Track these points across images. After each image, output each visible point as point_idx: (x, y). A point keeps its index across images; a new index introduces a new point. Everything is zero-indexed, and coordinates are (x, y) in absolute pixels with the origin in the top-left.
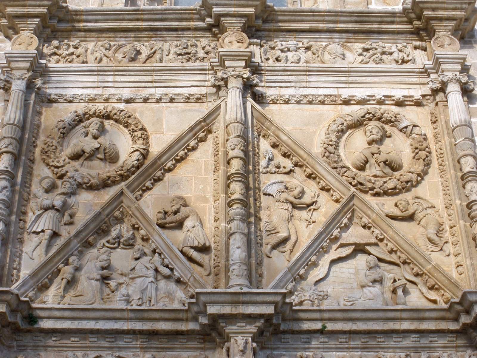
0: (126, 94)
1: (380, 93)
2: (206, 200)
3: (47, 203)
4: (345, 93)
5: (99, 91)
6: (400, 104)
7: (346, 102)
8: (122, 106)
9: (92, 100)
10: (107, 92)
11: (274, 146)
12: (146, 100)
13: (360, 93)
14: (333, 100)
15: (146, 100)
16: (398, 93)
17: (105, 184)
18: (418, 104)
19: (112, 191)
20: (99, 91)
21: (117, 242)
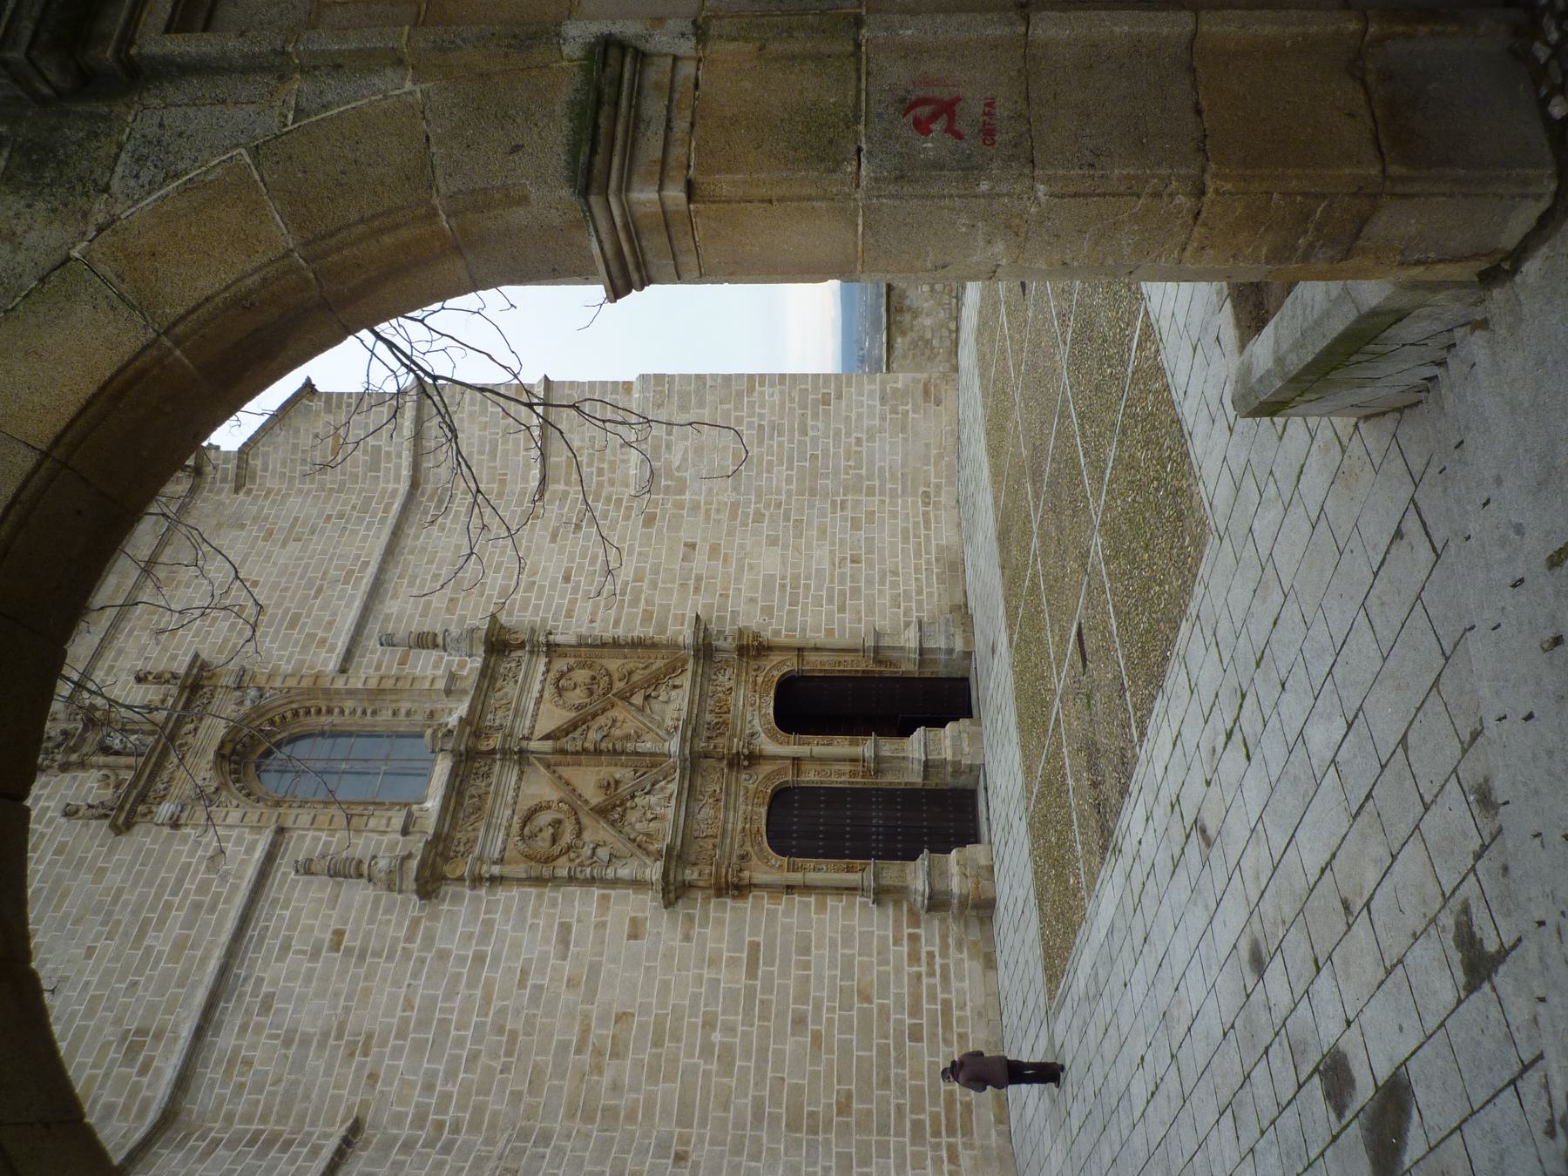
0: (508, 812)
1: (539, 677)
2: (599, 771)
3: (589, 853)
4: (536, 694)
5: (503, 829)
6: (548, 671)
7: (541, 697)
8: (516, 818)
9: (508, 835)
10: (505, 823)
11: (567, 735)
12: (515, 803)
13: (537, 687)
14: (539, 701)
15: (515, 803)
16: (542, 668)
17: (578, 822)
18: (550, 662)
19: (585, 820)
20: (503, 829)
21: (622, 816)
